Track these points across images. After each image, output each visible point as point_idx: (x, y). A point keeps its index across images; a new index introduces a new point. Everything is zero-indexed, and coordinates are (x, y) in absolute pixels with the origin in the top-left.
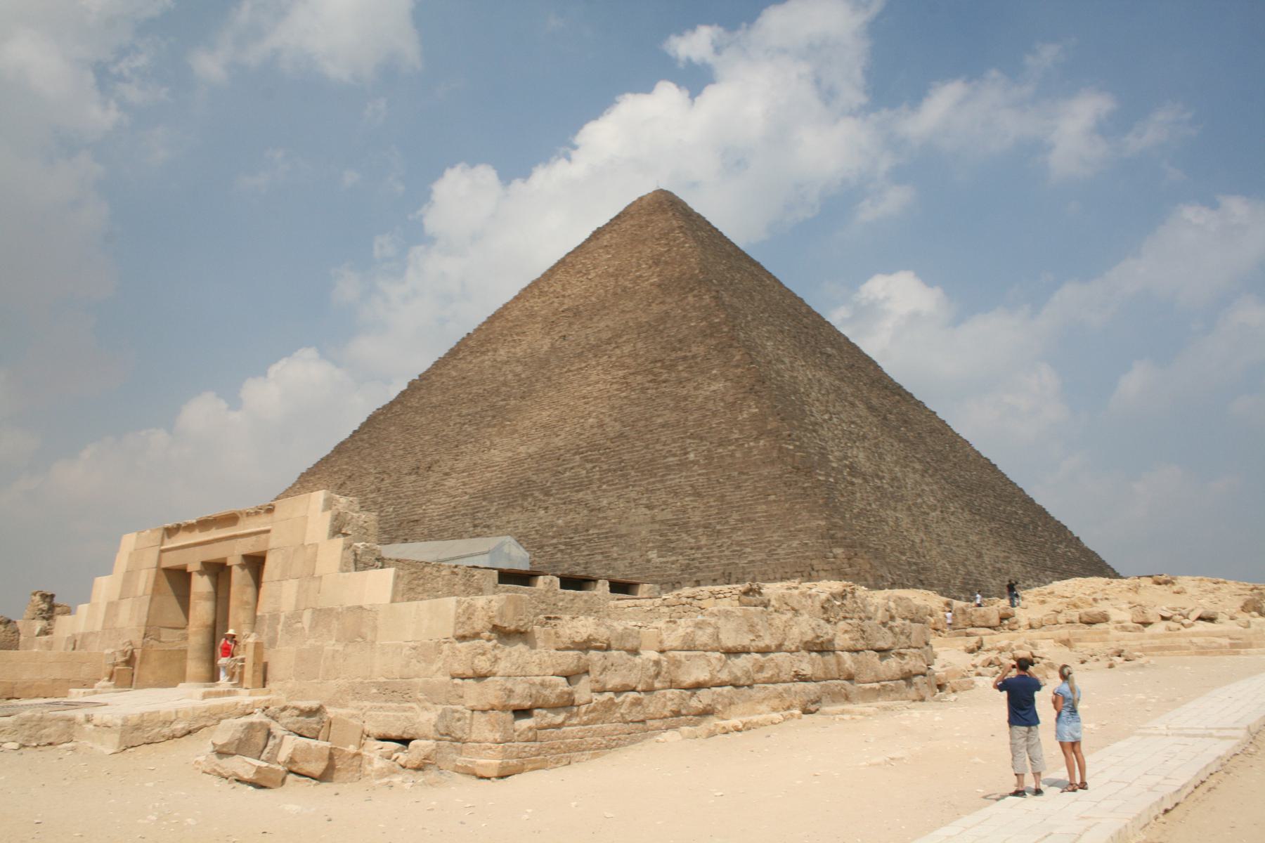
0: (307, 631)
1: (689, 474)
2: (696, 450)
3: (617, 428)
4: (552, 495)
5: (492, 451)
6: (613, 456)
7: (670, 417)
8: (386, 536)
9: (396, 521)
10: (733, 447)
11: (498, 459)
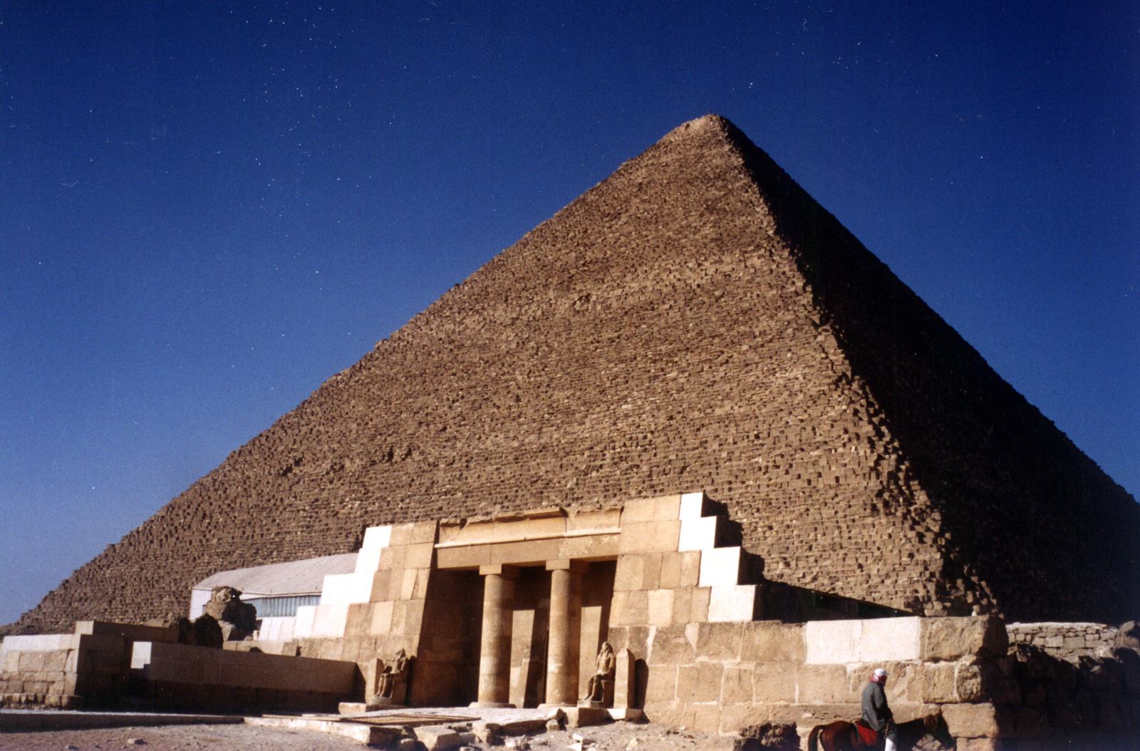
0: (695, 649)
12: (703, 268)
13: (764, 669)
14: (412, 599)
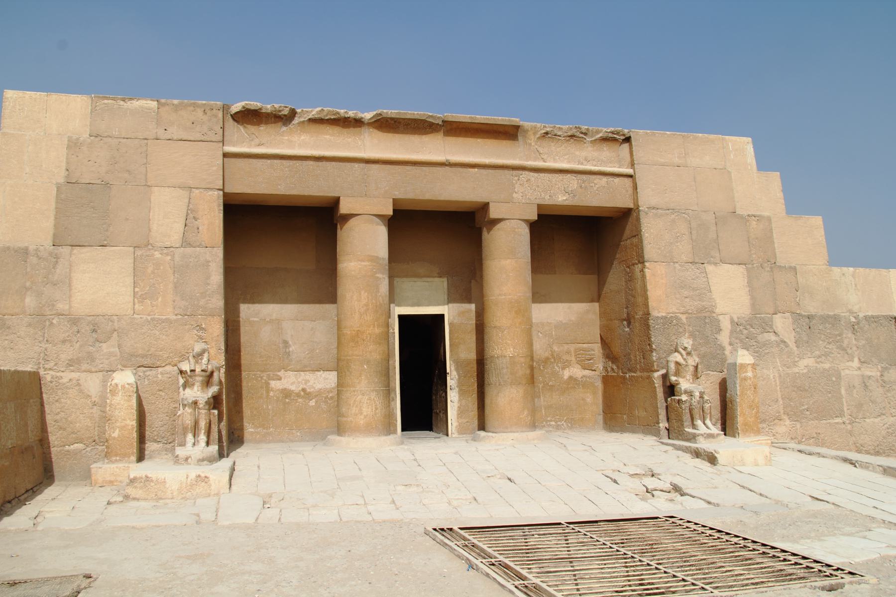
14: (186, 243)
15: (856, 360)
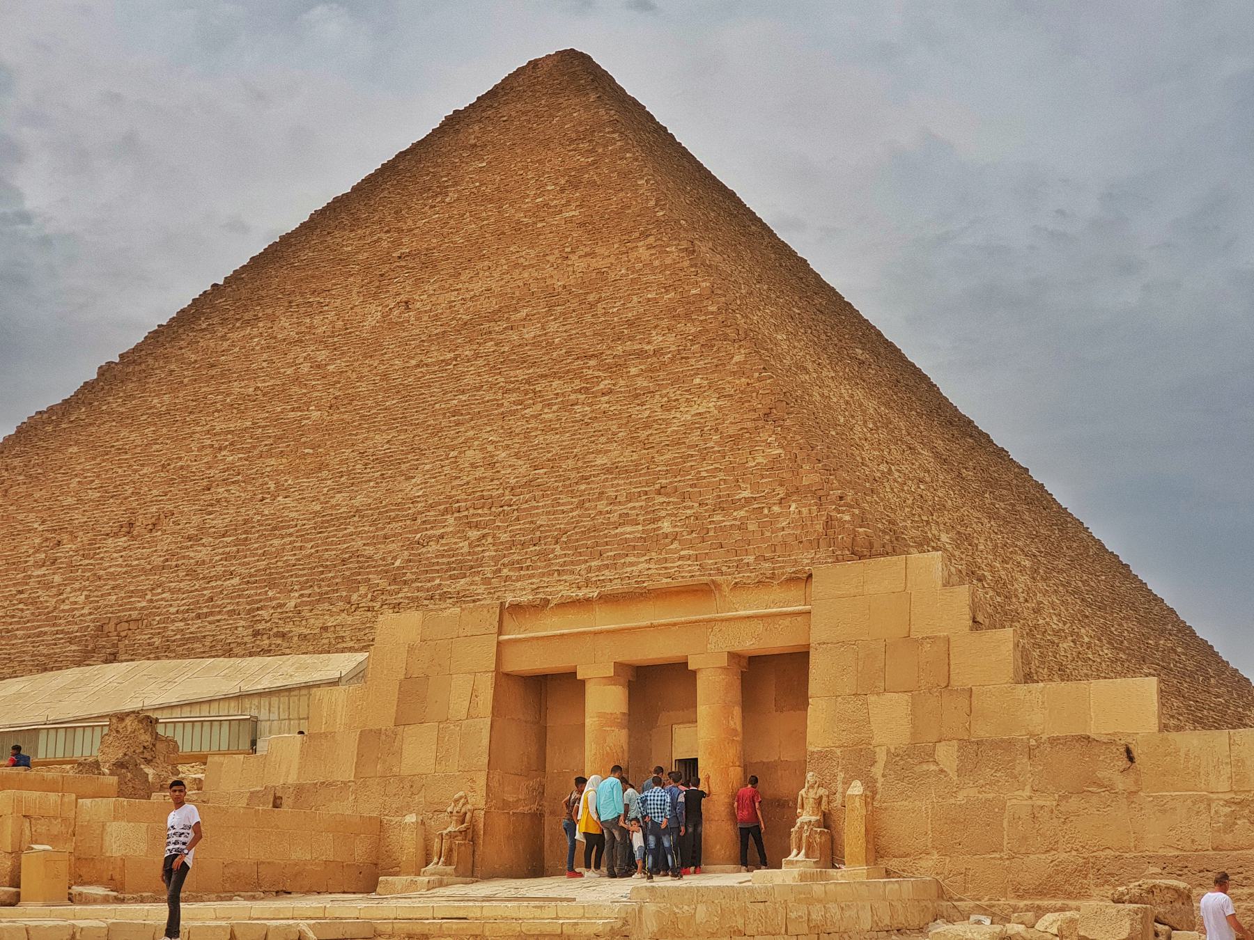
1: (664, 555)
2: (675, 515)
3: (523, 470)
4: (405, 582)
5: (280, 498)
6: (518, 519)
7: (627, 457)
8: (74, 648)
9: (93, 621)
10: (742, 513)
11: (292, 515)
12: (570, 263)
13: (1074, 803)
14: (469, 716)
15: (1028, 788)
